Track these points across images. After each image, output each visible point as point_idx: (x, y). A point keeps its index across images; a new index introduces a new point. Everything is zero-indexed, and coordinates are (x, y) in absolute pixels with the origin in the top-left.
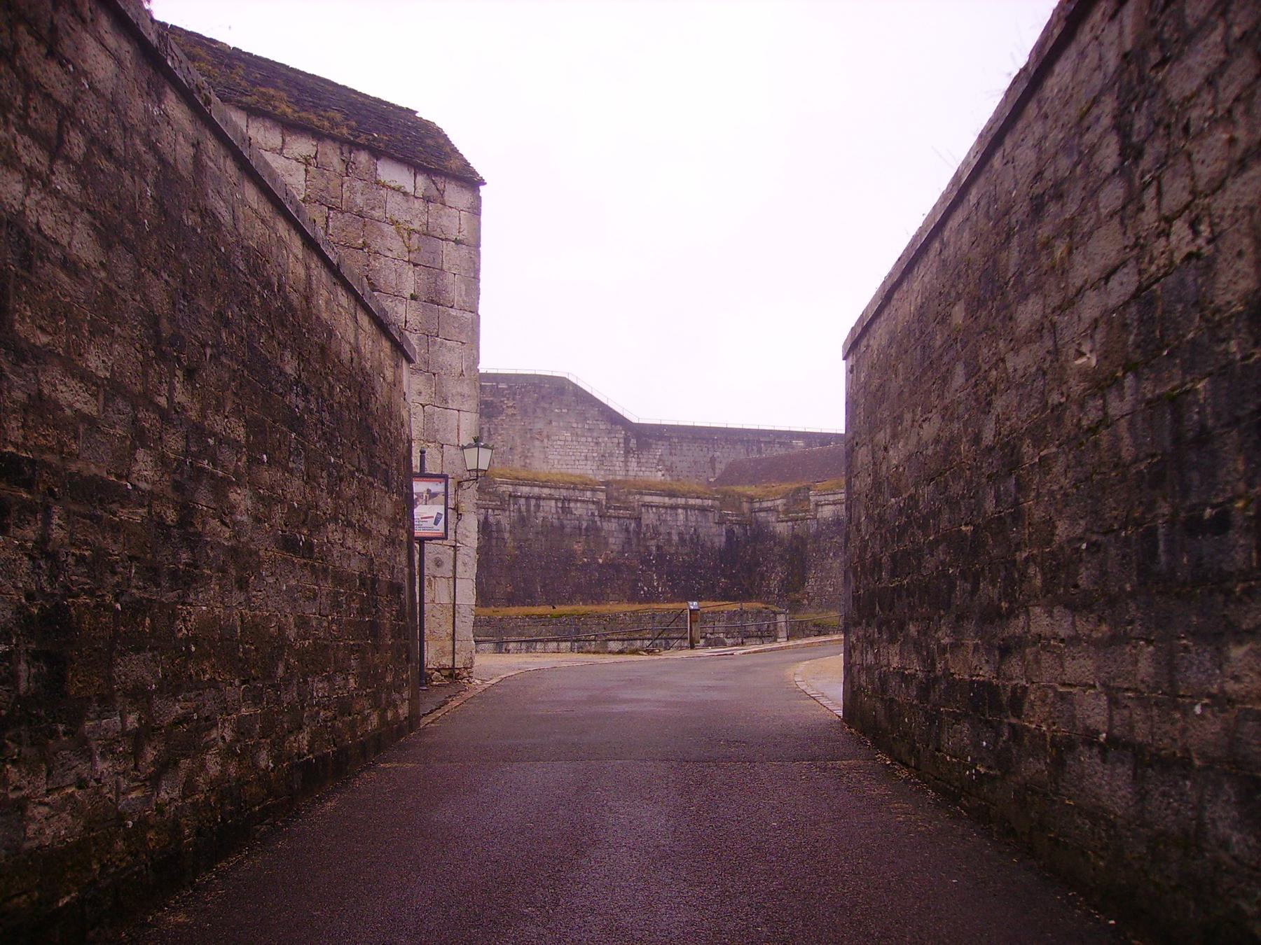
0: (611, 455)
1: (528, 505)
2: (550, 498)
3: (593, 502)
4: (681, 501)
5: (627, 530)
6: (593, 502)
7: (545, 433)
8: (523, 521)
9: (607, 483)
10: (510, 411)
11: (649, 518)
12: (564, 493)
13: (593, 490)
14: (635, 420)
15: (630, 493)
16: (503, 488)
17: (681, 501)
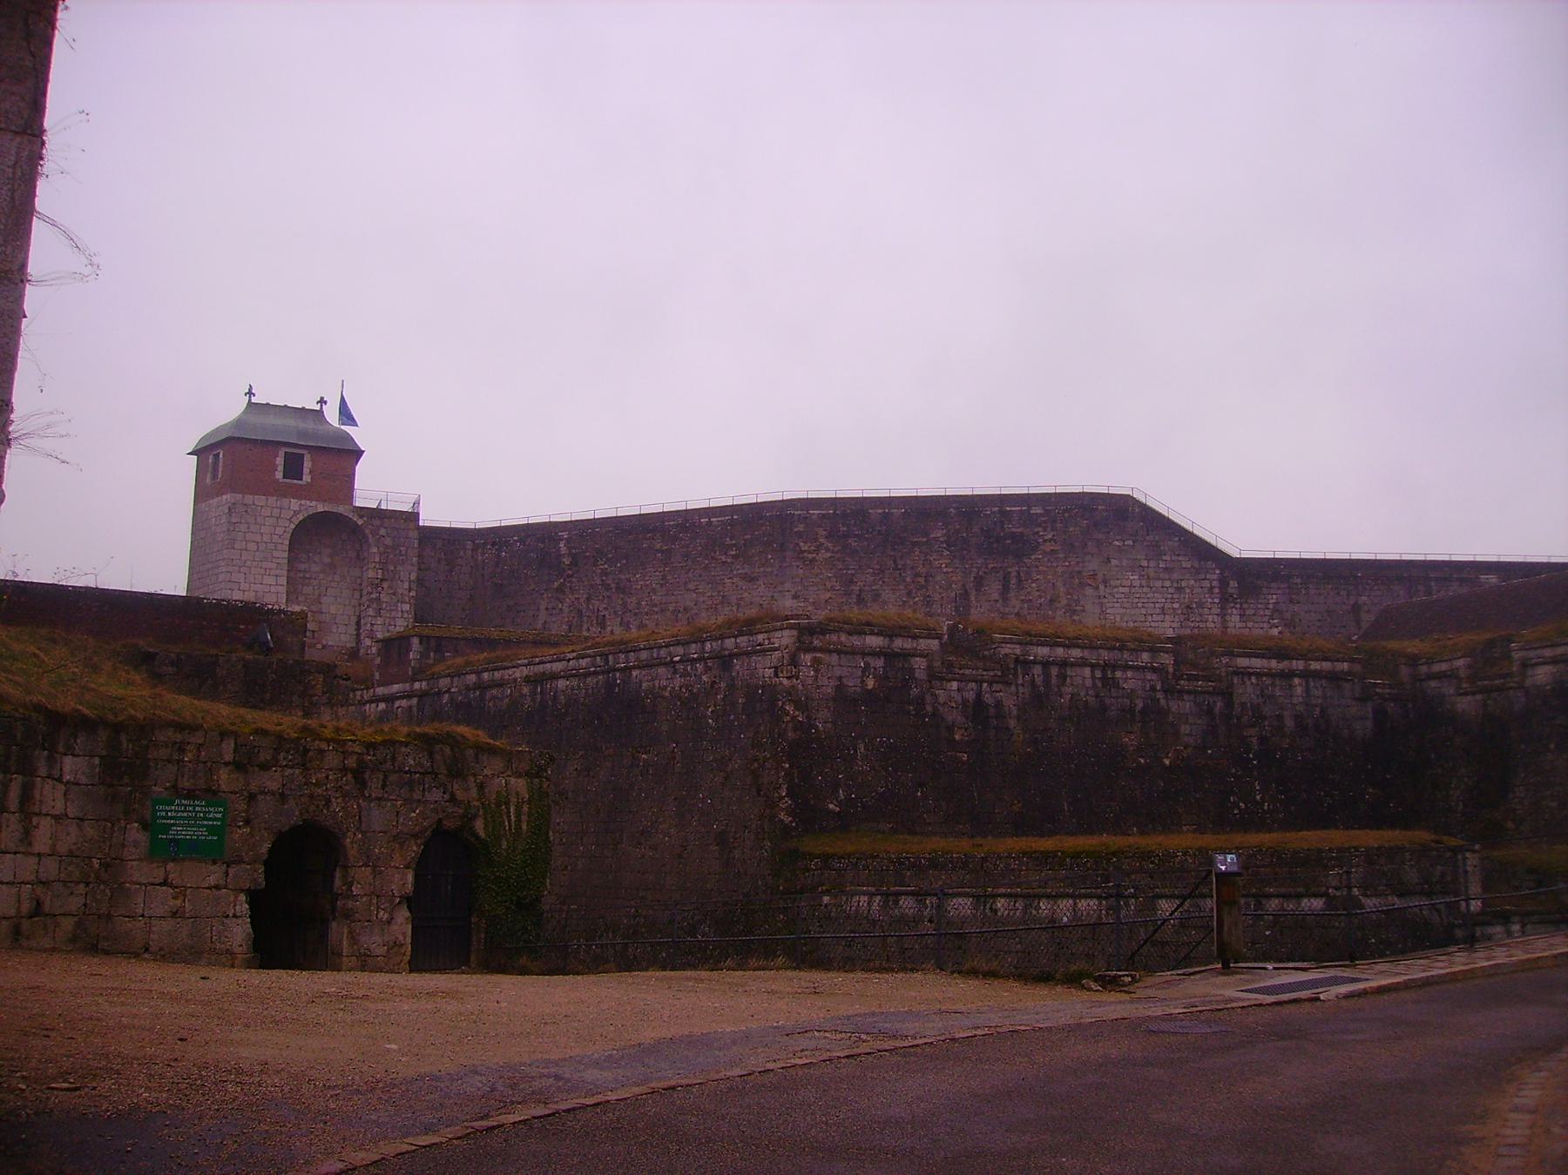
0: (1200, 605)
1: (1047, 676)
2: (1082, 663)
3: (1154, 670)
4: (1299, 665)
5: (1210, 712)
6: (1154, 670)
7: (1100, 577)
8: (1039, 699)
9: (1177, 641)
10: (1048, 547)
11: (1246, 692)
12: (1105, 655)
13: (1151, 650)
14: (1236, 555)
15: (1213, 653)
16: (1006, 649)
17: (1299, 665)
